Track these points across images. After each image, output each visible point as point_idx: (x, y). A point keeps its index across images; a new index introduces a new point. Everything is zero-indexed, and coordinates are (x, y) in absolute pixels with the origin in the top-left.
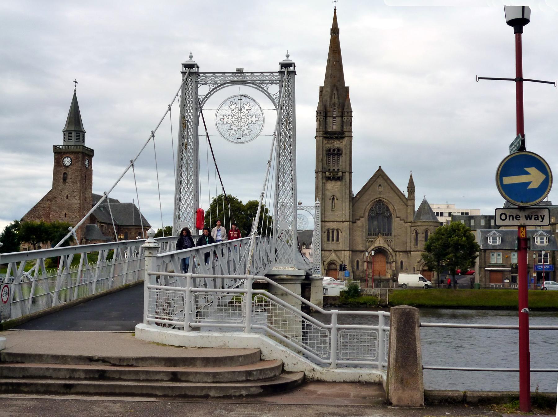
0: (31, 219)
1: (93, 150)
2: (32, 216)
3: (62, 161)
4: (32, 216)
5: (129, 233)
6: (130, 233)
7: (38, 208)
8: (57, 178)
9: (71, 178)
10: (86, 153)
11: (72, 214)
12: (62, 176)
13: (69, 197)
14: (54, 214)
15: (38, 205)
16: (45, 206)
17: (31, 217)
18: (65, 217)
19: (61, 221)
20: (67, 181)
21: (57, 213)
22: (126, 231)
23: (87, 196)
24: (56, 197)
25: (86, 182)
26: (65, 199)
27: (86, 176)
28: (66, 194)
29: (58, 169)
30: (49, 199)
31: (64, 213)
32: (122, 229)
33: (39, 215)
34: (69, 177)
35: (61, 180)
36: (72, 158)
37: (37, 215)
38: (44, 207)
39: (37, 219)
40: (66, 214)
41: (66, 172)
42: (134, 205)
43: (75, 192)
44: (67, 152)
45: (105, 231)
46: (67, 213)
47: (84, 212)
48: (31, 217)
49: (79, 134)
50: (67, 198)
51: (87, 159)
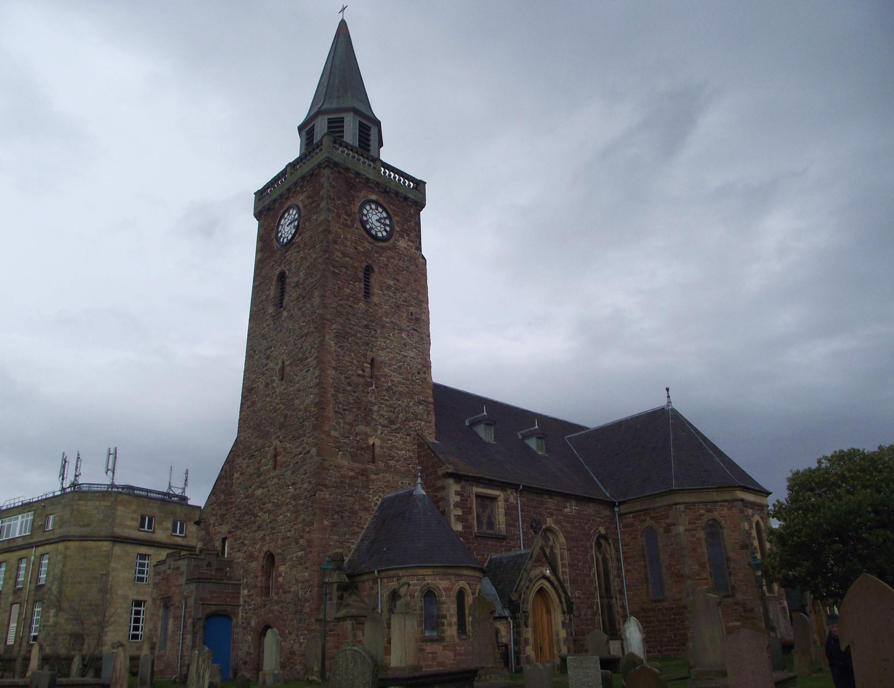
1: (420, 185)
5: (661, 530)
6: (667, 530)
10: (358, 174)
19: (259, 492)
22: (649, 522)
23: (382, 356)
25: (367, 294)
27: (368, 270)
28: (280, 362)
32: (629, 519)
34: (291, 280)
42: (673, 410)
44: (289, 190)
45: (511, 523)
47: (361, 428)
49: (343, 122)
50: (282, 379)
51: (378, 204)
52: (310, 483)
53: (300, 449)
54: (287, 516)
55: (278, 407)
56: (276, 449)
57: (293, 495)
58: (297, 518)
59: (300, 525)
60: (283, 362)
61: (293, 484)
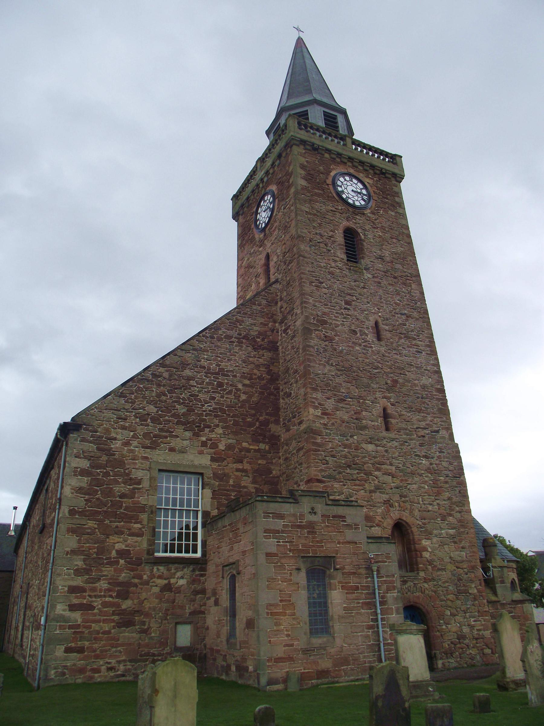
0: (141, 430)
2: (152, 409)
3: (329, 181)
4: (152, 409)
7: (187, 372)
8: (318, 238)
9: (381, 258)
11: (415, 417)
12: (340, 238)
13: (386, 335)
14: (330, 404)
15: (189, 357)
16: (227, 365)
17: (143, 418)
18: (387, 429)
19: (371, 447)
20: (365, 262)
21: (342, 400)
24: (325, 322)
26: (371, 337)
29: (317, 206)
30: (245, 337)
31: (377, 410)
33: (190, 410)
35: (341, 255)
36: (366, 183)
37: (181, 410)
38: (222, 372)
39: (179, 430)
40: (386, 416)
41: (351, 224)
43: (408, 317)
46: (391, 410)
48: (143, 418)
50: (379, 338)
52: (451, 464)
53: (423, 424)
54: (424, 488)
55: (380, 365)
56: (385, 410)
57: (429, 468)
58: (438, 494)
59: (444, 502)
60: (376, 323)
61: (426, 457)
